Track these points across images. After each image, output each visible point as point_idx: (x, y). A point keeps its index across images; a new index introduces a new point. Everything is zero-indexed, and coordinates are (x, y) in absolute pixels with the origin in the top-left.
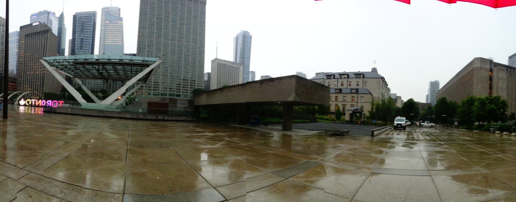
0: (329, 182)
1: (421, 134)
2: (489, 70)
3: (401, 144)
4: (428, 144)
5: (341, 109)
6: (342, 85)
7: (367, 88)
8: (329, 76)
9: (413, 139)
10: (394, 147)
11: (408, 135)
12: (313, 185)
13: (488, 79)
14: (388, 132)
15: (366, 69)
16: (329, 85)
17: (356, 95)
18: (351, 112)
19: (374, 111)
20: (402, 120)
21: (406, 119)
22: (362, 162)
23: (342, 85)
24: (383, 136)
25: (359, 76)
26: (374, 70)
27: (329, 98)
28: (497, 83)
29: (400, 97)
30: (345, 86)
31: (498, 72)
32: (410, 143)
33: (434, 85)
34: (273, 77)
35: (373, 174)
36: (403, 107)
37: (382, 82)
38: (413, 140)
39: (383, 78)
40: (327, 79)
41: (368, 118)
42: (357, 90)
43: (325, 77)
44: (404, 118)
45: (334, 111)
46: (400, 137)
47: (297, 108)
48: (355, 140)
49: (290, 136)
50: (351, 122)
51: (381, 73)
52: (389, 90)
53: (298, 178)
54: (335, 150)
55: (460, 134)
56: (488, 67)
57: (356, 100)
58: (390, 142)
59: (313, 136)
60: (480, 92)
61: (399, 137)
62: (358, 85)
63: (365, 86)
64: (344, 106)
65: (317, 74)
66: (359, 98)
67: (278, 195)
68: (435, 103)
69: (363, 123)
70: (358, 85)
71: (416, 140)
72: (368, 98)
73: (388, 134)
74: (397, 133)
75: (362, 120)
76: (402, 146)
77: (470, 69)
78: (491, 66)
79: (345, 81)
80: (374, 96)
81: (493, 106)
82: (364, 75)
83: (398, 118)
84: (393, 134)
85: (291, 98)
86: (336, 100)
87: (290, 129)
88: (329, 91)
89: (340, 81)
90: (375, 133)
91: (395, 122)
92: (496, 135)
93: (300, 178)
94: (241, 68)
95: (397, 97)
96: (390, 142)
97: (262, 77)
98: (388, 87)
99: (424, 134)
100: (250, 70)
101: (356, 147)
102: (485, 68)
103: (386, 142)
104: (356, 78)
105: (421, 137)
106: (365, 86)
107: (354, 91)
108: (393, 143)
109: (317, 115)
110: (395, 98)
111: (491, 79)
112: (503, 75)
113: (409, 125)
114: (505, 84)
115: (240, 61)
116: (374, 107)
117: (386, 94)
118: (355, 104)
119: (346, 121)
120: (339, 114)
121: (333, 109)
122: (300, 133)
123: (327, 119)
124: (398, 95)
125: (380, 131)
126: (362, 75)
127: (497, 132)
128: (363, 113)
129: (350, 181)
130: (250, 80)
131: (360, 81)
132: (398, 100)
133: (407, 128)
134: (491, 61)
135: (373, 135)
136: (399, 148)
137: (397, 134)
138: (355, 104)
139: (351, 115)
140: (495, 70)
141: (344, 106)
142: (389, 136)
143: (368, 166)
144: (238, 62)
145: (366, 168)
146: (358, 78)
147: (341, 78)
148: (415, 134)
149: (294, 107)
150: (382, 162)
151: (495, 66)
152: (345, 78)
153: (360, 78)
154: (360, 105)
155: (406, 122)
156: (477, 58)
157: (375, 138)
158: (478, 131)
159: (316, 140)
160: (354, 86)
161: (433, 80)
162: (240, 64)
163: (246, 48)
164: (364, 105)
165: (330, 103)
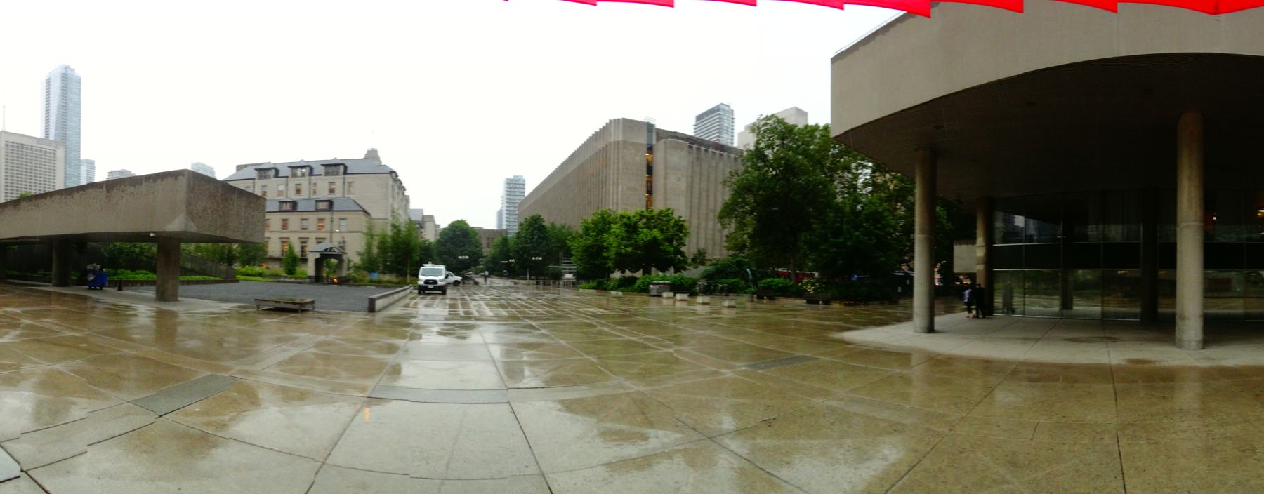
0: (266, 423)
1: (488, 305)
2: (645, 149)
3: (436, 329)
4: (503, 328)
5: (297, 250)
6: (298, 192)
7: (353, 197)
8: (263, 171)
9: (468, 316)
10: (420, 337)
11: (452, 306)
12: (223, 434)
13: (645, 169)
14: (407, 301)
15: (350, 151)
16: (265, 193)
17: (327, 216)
18: (318, 256)
19: (375, 251)
20: (438, 273)
21: (447, 269)
22: (344, 374)
23: (298, 192)
24: (396, 311)
25: (333, 169)
26: (372, 155)
27: (264, 224)
28: (666, 178)
29: (432, 217)
30: (304, 195)
31: (665, 153)
32: (458, 326)
33: (514, 185)
34: (138, 173)
35: (372, 400)
36: (439, 242)
37: (391, 182)
38: (469, 318)
39: (393, 173)
40: (260, 178)
41: (357, 268)
42: (331, 203)
43: (254, 174)
44: (442, 267)
45: (277, 254)
46: (432, 312)
47: (192, 247)
48: (328, 321)
49: (174, 315)
50: (318, 279)
51: (387, 160)
52: (406, 200)
53: (187, 414)
54: (280, 347)
55: (580, 302)
56: (642, 140)
57: (327, 228)
58: (409, 325)
59: (228, 315)
60: (624, 200)
61: (430, 311)
62: (332, 191)
63: (349, 193)
64: (304, 242)
65: (239, 168)
67: (145, 456)
68: (515, 229)
69: (343, 281)
70: (332, 191)
71: (477, 319)
72: (358, 222)
73: (407, 306)
74: (425, 302)
75: (344, 273)
76: (441, 333)
77: (600, 145)
78: (650, 138)
79: (304, 183)
80: (374, 216)
81: (656, 233)
82: (346, 167)
83: (429, 266)
84: (416, 305)
85: (176, 225)
86: (285, 227)
87: (173, 298)
88: (264, 206)
89: (292, 183)
90: (379, 304)
91: (420, 277)
92: (665, 302)
93: (192, 416)
94: (60, 153)
95: (424, 217)
96: (409, 325)
97: (111, 173)
98: (406, 193)
99: (495, 303)
100: (83, 157)
101: (331, 337)
102: (633, 144)
103: (403, 326)
104: (327, 174)
105: (488, 312)
106: (349, 193)
107: (323, 206)
108: (418, 327)
109: (237, 266)
110: (419, 219)
111: (650, 170)
112: (680, 158)
113: (456, 283)
114: (684, 180)
115: (56, 135)
116: (375, 243)
117: (401, 211)
118: (327, 236)
119: (310, 277)
120: (292, 262)
121: (274, 249)
122: (199, 308)
123: (260, 275)
124: (426, 213)
125: (391, 299)
126: (342, 168)
127: (665, 294)
128: (345, 257)
129: (319, 419)
130: (84, 182)
131: (338, 180)
132: (428, 225)
133: (449, 291)
134: (650, 127)
135: (372, 309)
136: (432, 339)
137: (427, 306)
138: (327, 236)
139: (319, 263)
140: (660, 147)
141: (304, 242)
142: (410, 310)
143: (360, 382)
144: (52, 137)
145: (355, 388)
146: (332, 174)
147: (294, 175)
148: (473, 303)
149: (183, 245)
150: (396, 371)
151: (659, 139)
152: (303, 175)
153: (337, 174)
154: (337, 238)
155: (447, 276)
156: (617, 121)
157: (379, 317)
158: (620, 293)
159: (234, 325)
160: (323, 194)
161: (511, 177)
162: (57, 143)
163: (71, 105)
164: (348, 237)
165: (267, 235)
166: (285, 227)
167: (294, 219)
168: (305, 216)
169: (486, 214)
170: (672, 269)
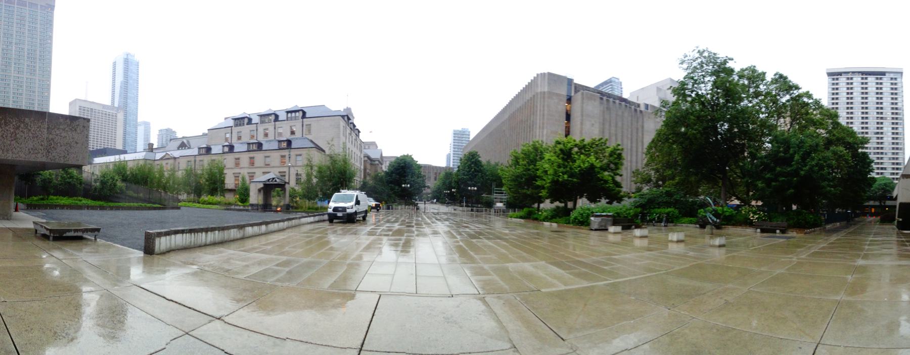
2: (565, 99)
7: (310, 137)
13: (564, 116)
17: (286, 153)
28: (582, 124)
31: (583, 103)
42: (289, 142)
56: (563, 92)
66: (293, 157)
68: (454, 165)
77: (528, 96)
78: (569, 90)
102: (558, 95)
111: (568, 117)
112: (594, 107)
114: (597, 125)
134: (570, 81)
140: (577, 98)
151: (576, 92)
156: (543, 75)
166: (237, 165)
167: (259, 157)
168: (267, 154)
169: (435, 153)
170: (604, 201)
